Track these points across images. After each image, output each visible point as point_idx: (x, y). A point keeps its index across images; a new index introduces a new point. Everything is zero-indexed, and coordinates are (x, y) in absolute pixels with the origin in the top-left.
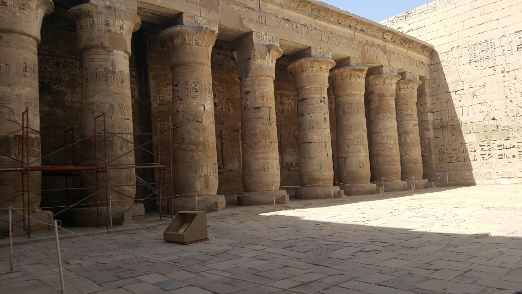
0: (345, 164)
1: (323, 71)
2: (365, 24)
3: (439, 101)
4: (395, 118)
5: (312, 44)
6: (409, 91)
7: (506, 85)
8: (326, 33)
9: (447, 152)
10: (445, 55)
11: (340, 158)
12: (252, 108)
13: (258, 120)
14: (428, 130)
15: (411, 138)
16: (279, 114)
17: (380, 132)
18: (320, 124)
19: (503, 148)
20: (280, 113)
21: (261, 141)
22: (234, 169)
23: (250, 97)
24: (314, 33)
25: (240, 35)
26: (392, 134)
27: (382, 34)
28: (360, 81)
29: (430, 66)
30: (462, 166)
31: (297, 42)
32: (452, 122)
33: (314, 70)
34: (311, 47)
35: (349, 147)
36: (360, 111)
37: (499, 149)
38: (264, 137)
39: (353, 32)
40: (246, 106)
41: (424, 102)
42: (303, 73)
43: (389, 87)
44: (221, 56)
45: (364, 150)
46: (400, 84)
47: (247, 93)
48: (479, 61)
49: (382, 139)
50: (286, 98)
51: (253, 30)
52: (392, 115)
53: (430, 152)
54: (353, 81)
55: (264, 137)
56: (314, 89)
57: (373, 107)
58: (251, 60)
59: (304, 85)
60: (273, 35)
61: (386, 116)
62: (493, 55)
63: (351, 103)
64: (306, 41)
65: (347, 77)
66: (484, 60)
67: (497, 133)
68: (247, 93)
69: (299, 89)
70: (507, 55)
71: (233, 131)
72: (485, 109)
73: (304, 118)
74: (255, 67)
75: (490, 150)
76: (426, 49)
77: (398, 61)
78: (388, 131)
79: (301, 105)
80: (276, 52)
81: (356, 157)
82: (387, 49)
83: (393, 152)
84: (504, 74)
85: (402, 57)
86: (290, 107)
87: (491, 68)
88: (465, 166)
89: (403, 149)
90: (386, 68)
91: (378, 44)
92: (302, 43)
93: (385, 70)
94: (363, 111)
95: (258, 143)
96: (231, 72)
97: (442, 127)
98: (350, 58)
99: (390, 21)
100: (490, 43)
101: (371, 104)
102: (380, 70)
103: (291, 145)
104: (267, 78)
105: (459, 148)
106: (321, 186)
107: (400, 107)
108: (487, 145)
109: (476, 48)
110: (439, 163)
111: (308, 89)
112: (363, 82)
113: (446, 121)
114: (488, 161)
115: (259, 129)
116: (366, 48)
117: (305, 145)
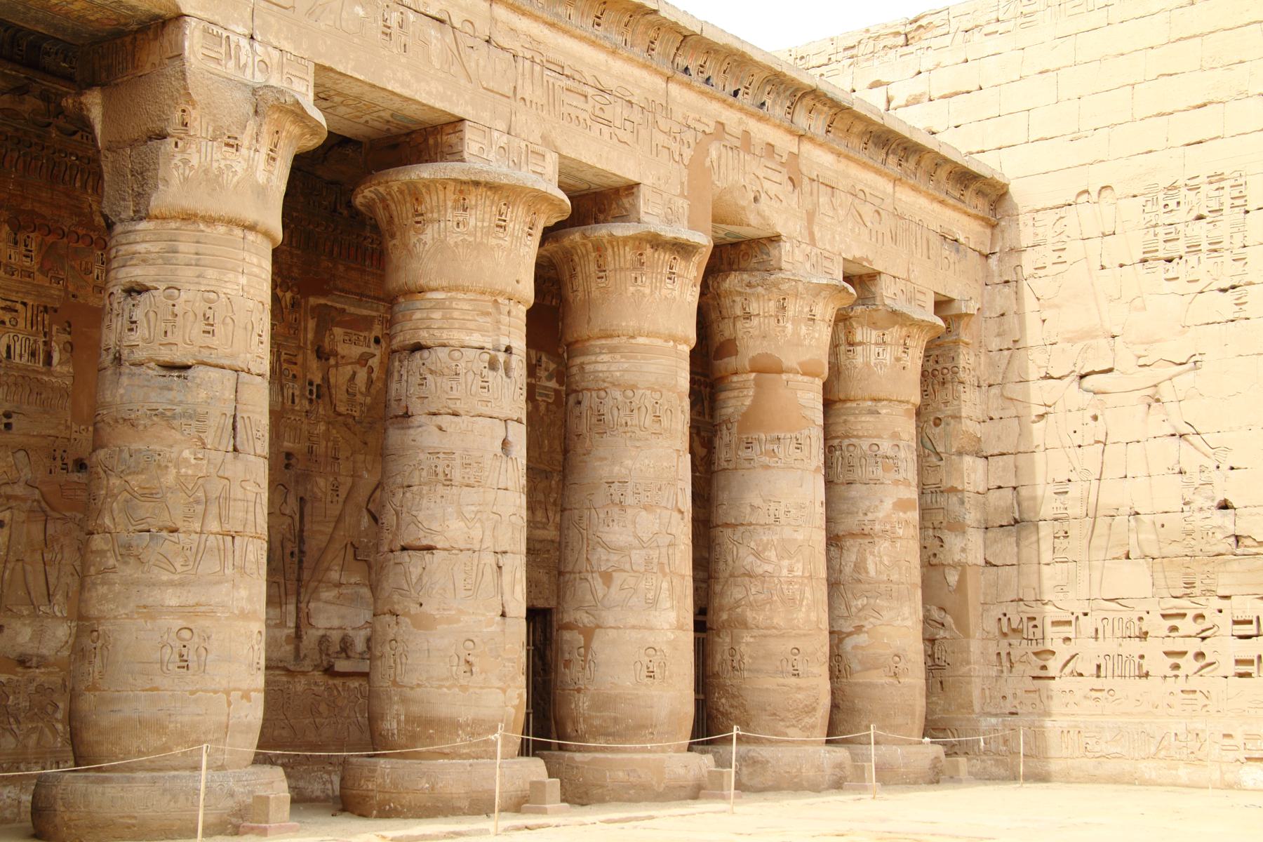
0: (586, 656)
1: (509, 229)
2: (716, 52)
3: (1013, 412)
4: (818, 468)
5: (469, 109)
6: (887, 357)
8: (537, 68)
9: (1031, 630)
10: (1051, 216)
11: (569, 627)
12: (152, 364)
13: (176, 423)
14: (958, 527)
15: (881, 562)
16: (306, 403)
17: (750, 524)
18: (482, 469)
19: (1254, 632)
20: (311, 401)
21: (180, 524)
22: (45, 652)
23: (146, 314)
24: (482, 62)
25: (123, 21)
26: (800, 536)
27: (788, 104)
28: (676, 293)
29: (987, 257)
31: (398, 90)
33: (472, 222)
34: (462, 120)
35: (607, 578)
36: (665, 422)
37: (1241, 637)
38: (200, 509)
39: (660, 83)
40: (125, 352)
41: (949, 410)
42: (417, 232)
43: (804, 330)
44: (30, 104)
45: (671, 596)
46: (854, 324)
47: (135, 290)
48: (1181, 258)
49: (757, 555)
50: (346, 334)
51: (184, 12)
52: (807, 454)
54: (647, 291)
55: (200, 509)
56: (467, 307)
57: (731, 410)
58: (170, 140)
59: (422, 282)
60: (287, 46)
61: (781, 456)
62: (1238, 241)
63: (633, 388)
64: (441, 89)
65: (621, 269)
66: (1203, 256)
67: (1235, 566)
68: (135, 290)
69: (401, 300)
71: (59, 463)
72: (1190, 457)
73: (412, 431)
74: (186, 179)
75: (1204, 639)
76: (972, 187)
77: (850, 226)
78: (783, 519)
79: (404, 372)
80: (294, 122)
81: (634, 627)
82: (804, 170)
83: (801, 615)
85: (867, 211)
86: (362, 374)
87: (1224, 290)
89: (848, 607)
90: (796, 251)
91: (770, 145)
92: (423, 98)
93: (791, 256)
94: (680, 427)
95: (165, 534)
96: (78, 184)
97: (1016, 522)
98: (639, 191)
99: (841, 49)
100: (1228, 189)
101: (723, 395)
102: (768, 254)
103: (350, 551)
104: (238, 232)
105: (1081, 617)
106: (461, 756)
107: (845, 422)
109: (1172, 205)
110: (998, 677)
111: (439, 305)
112: (689, 298)
114: (1194, 683)
115: (177, 466)
116: (714, 153)
117: (407, 559)
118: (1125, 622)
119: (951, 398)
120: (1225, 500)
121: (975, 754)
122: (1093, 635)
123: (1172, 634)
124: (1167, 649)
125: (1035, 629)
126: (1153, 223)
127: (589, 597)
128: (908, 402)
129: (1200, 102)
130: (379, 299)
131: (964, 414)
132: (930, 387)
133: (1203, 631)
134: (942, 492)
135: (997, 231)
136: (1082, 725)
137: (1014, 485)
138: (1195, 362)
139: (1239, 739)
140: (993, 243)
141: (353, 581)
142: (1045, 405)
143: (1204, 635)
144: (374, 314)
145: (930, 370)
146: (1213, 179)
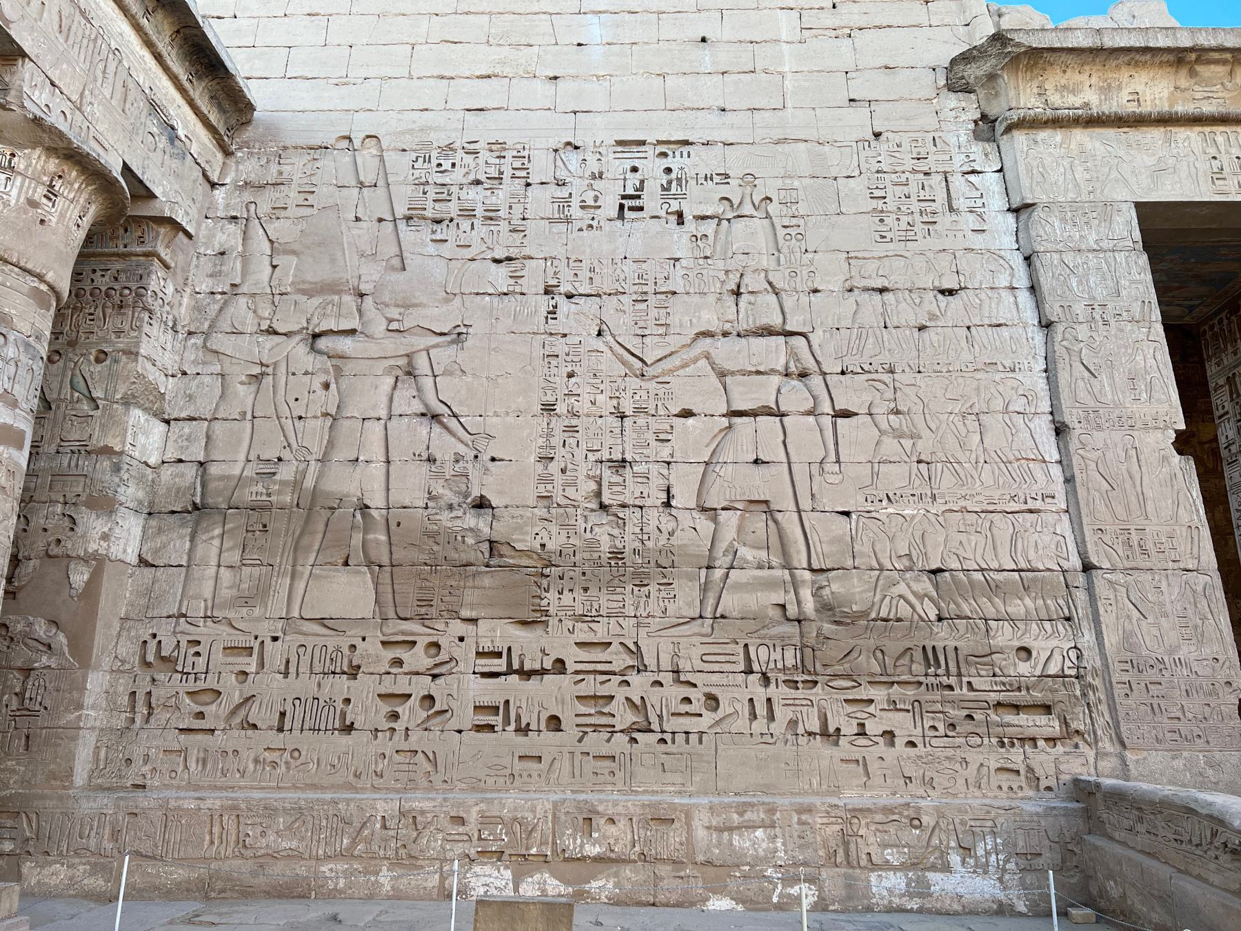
3: (217, 368)
7: (556, 351)
9: (190, 659)
14: (105, 505)
19: (504, 669)
30: (256, 761)
32: (260, 488)
37: (485, 675)
41: (122, 343)
48: (451, 220)
53: (81, 649)
62: (517, 211)
67: (487, 581)
70: (577, 225)
72: (444, 445)
75: (435, 676)
84: (552, 302)
88: (274, 764)
100: (509, 159)
105: (268, 641)
108: (422, 642)
109: (447, 165)
113: (222, 478)
118: (329, 651)
119: (127, 328)
120: (482, 497)
121: (61, 854)
122: (282, 668)
123: (393, 670)
124: (383, 691)
125: (195, 659)
126: (423, 180)
128: (40, 277)
129: (484, 73)
131: (142, 351)
132: (100, 310)
133: (436, 665)
134: (89, 453)
135: (231, 162)
136: (243, 806)
137: (201, 458)
138: (459, 334)
139: (472, 828)
140: (223, 173)
142: (262, 364)
143: (436, 671)
145: (104, 289)
146: (494, 147)
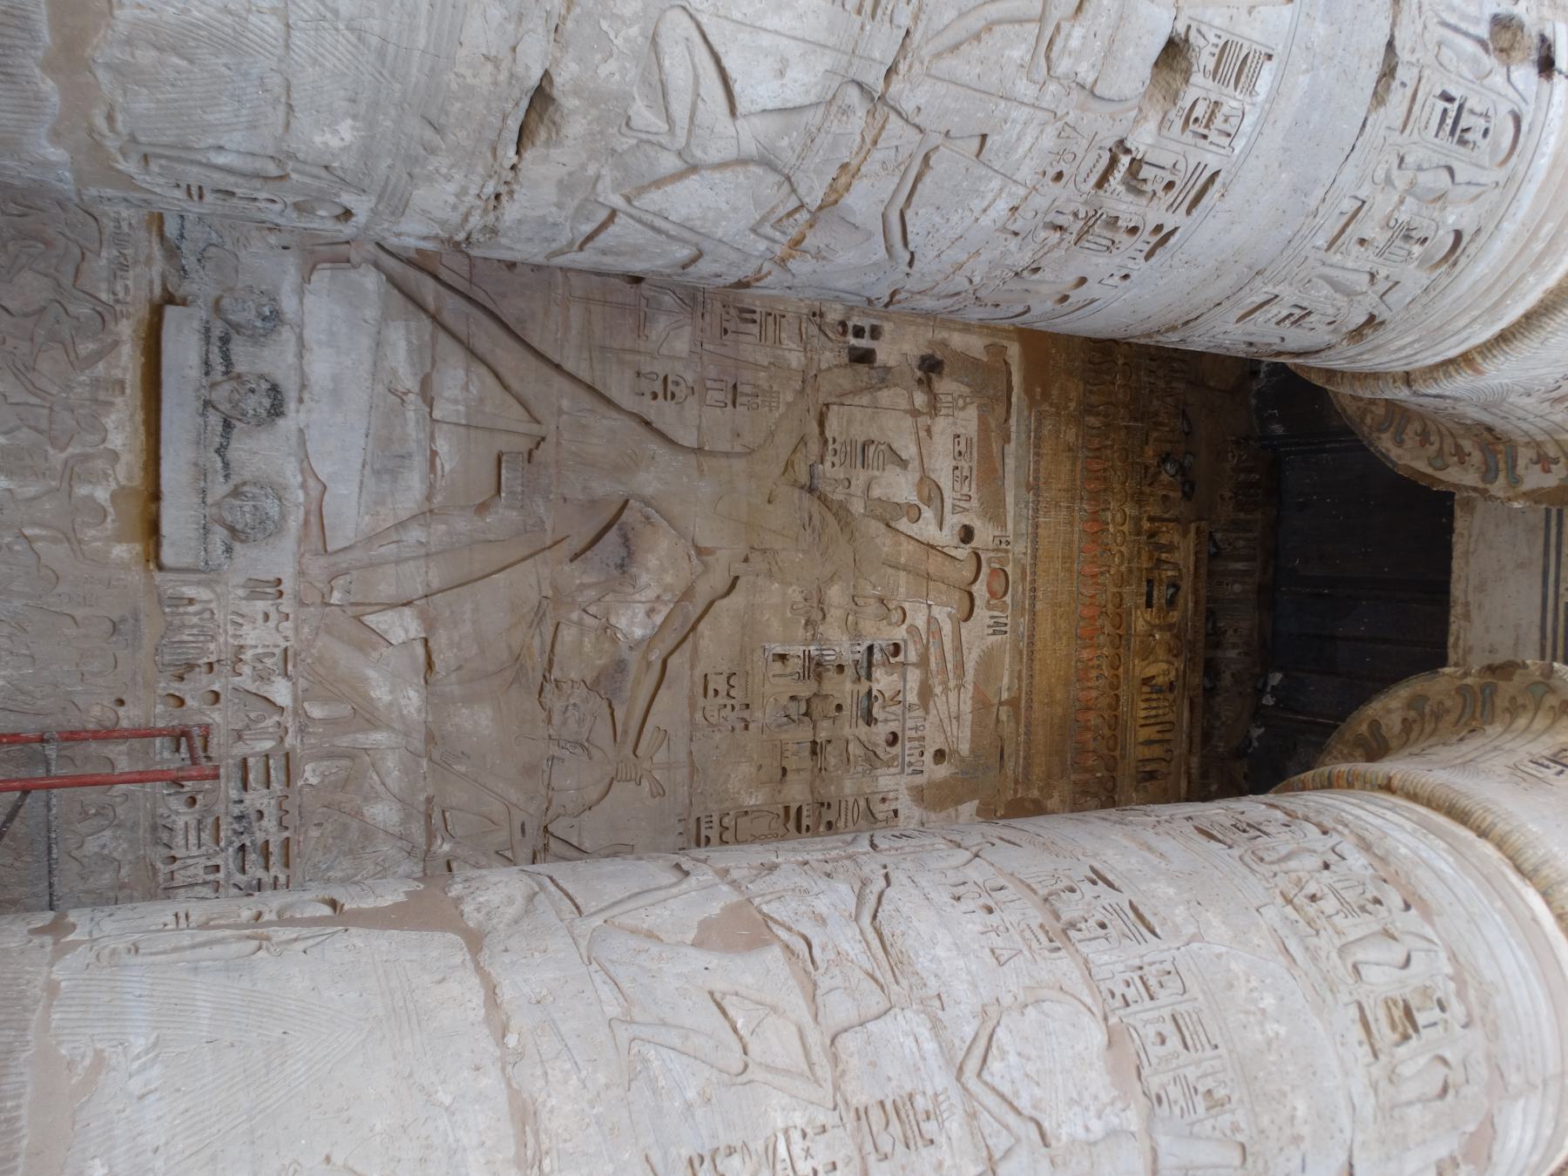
81: (524, 1115)
127: (615, 890)
130: (1035, 541)
141: (442, 446)
144: (1010, 526)
